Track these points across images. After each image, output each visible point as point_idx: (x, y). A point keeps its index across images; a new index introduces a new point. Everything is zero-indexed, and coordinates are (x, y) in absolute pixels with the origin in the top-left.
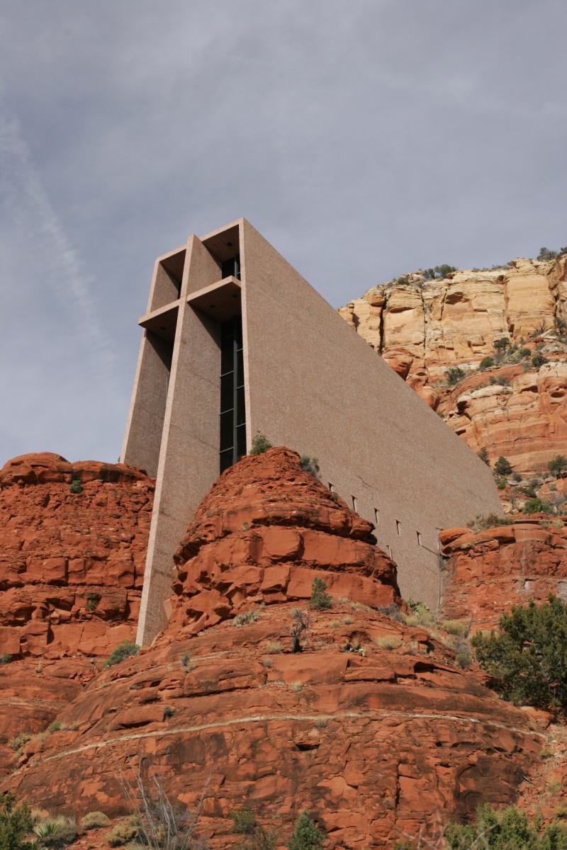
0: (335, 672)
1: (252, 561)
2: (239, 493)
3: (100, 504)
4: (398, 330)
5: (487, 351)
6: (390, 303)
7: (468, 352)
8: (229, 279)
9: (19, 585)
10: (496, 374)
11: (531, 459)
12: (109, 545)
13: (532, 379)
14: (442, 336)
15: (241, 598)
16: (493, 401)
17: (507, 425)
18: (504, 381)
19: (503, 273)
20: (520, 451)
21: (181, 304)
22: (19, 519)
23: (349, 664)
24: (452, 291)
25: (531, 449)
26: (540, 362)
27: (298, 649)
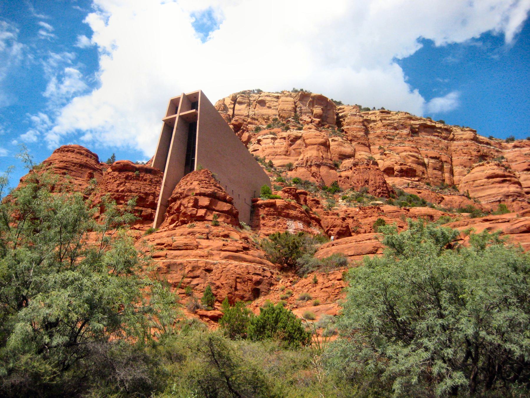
0: (219, 247)
2: (191, 184)
3: (145, 180)
4: (240, 110)
6: (238, 100)
7: (264, 123)
8: (194, 110)
10: (272, 131)
11: (280, 163)
13: (285, 134)
14: (255, 115)
16: (269, 140)
17: (274, 150)
19: (279, 95)
21: (177, 116)
22: (118, 182)
23: (224, 245)
24: (260, 99)
26: (287, 129)
27: (208, 238)
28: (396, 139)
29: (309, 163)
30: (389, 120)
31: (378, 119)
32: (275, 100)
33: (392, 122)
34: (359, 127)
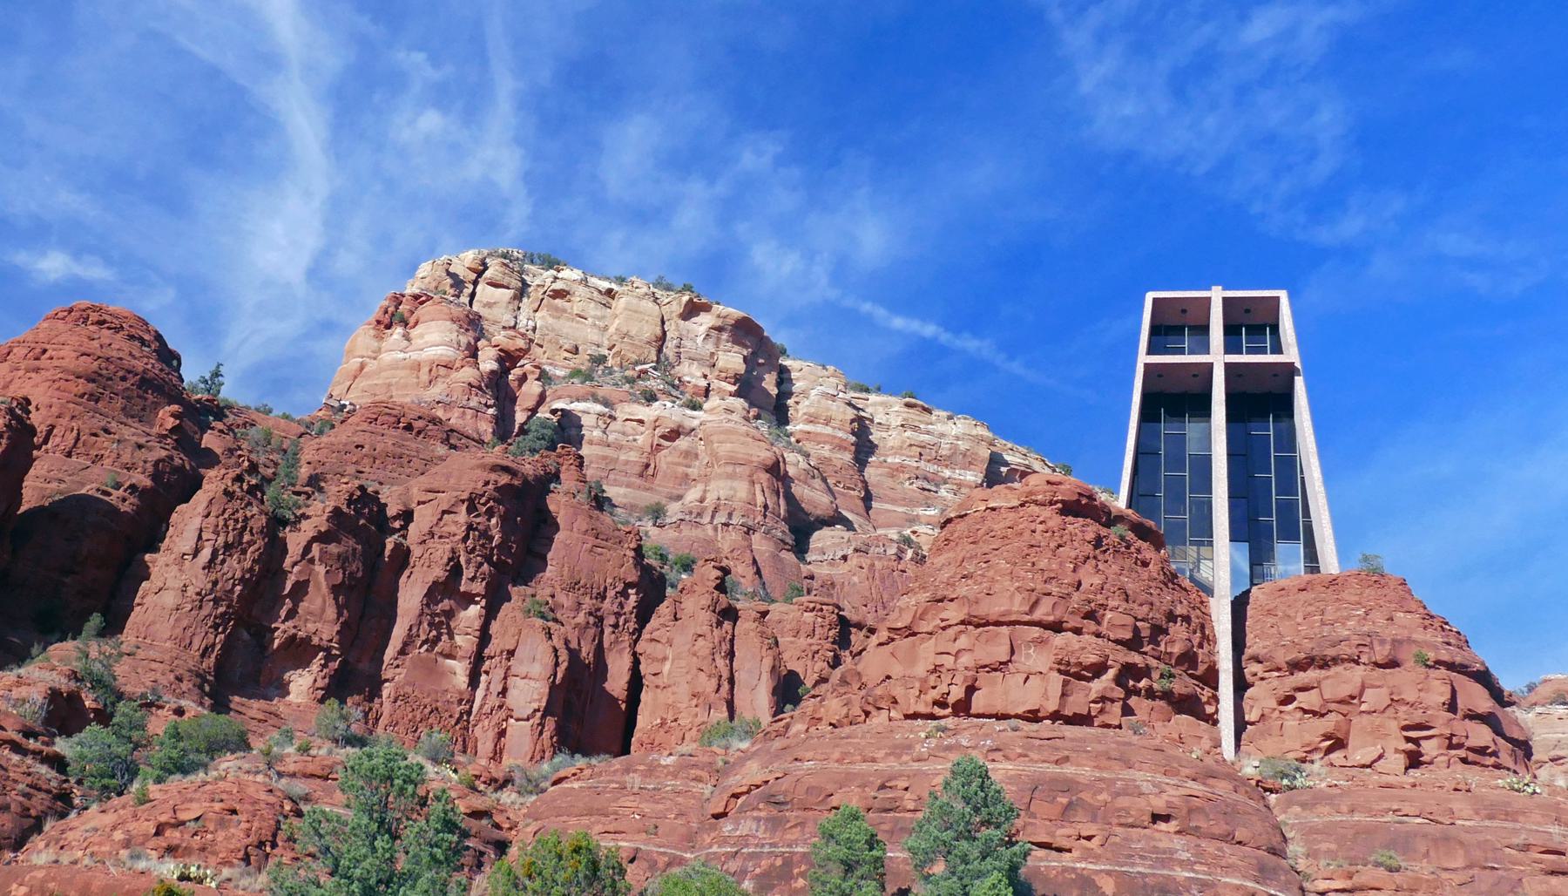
1: (1452, 706)
3: (1145, 564)
4: (489, 305)
5: (581, 362)
9: (1078, 631)
10: (601, 392)
11: (625, 496)
12: (1171, 617)
15: (1439, 747)
18: (606, 403)
20: (616, 483)
24: (558, 285)
25: (628, 486)
28: (943, 492)
29: (721, 518)
30: (928, 433)
31: (896, 421)
32: (605, 299)
33: (934, 440)
34: (840, 434)
